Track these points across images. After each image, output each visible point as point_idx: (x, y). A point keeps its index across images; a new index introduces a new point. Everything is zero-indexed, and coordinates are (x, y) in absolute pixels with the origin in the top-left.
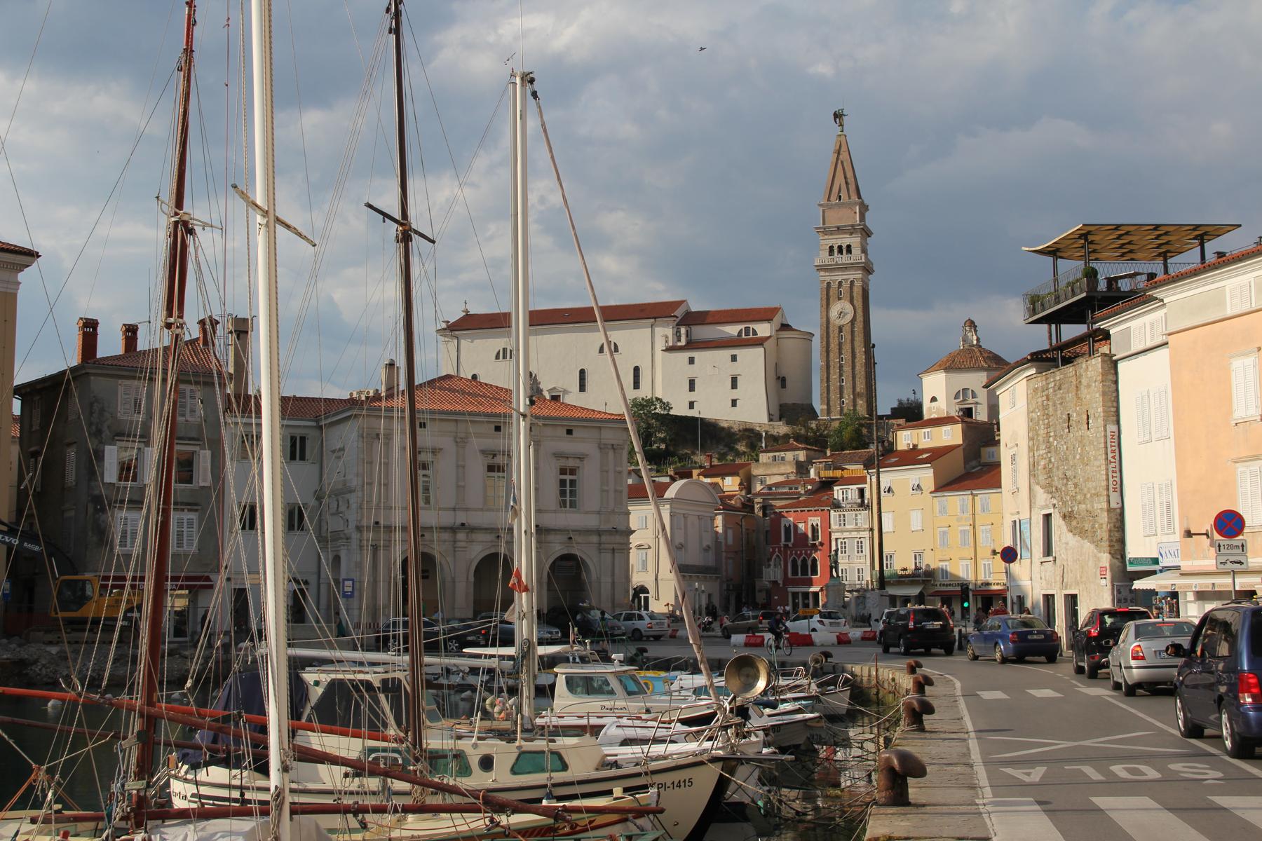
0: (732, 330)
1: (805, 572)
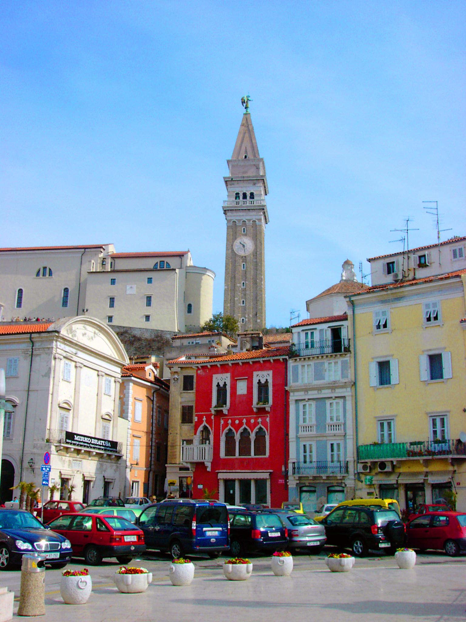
0: (150, 263)
1: (245, 450)
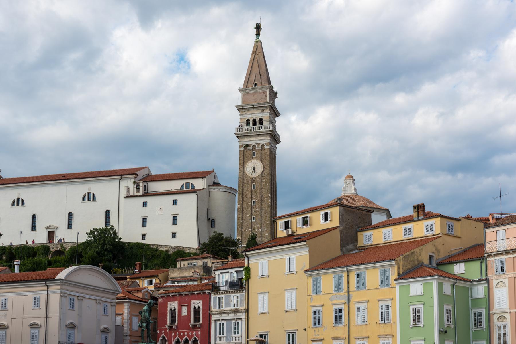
0: (176, 185)
